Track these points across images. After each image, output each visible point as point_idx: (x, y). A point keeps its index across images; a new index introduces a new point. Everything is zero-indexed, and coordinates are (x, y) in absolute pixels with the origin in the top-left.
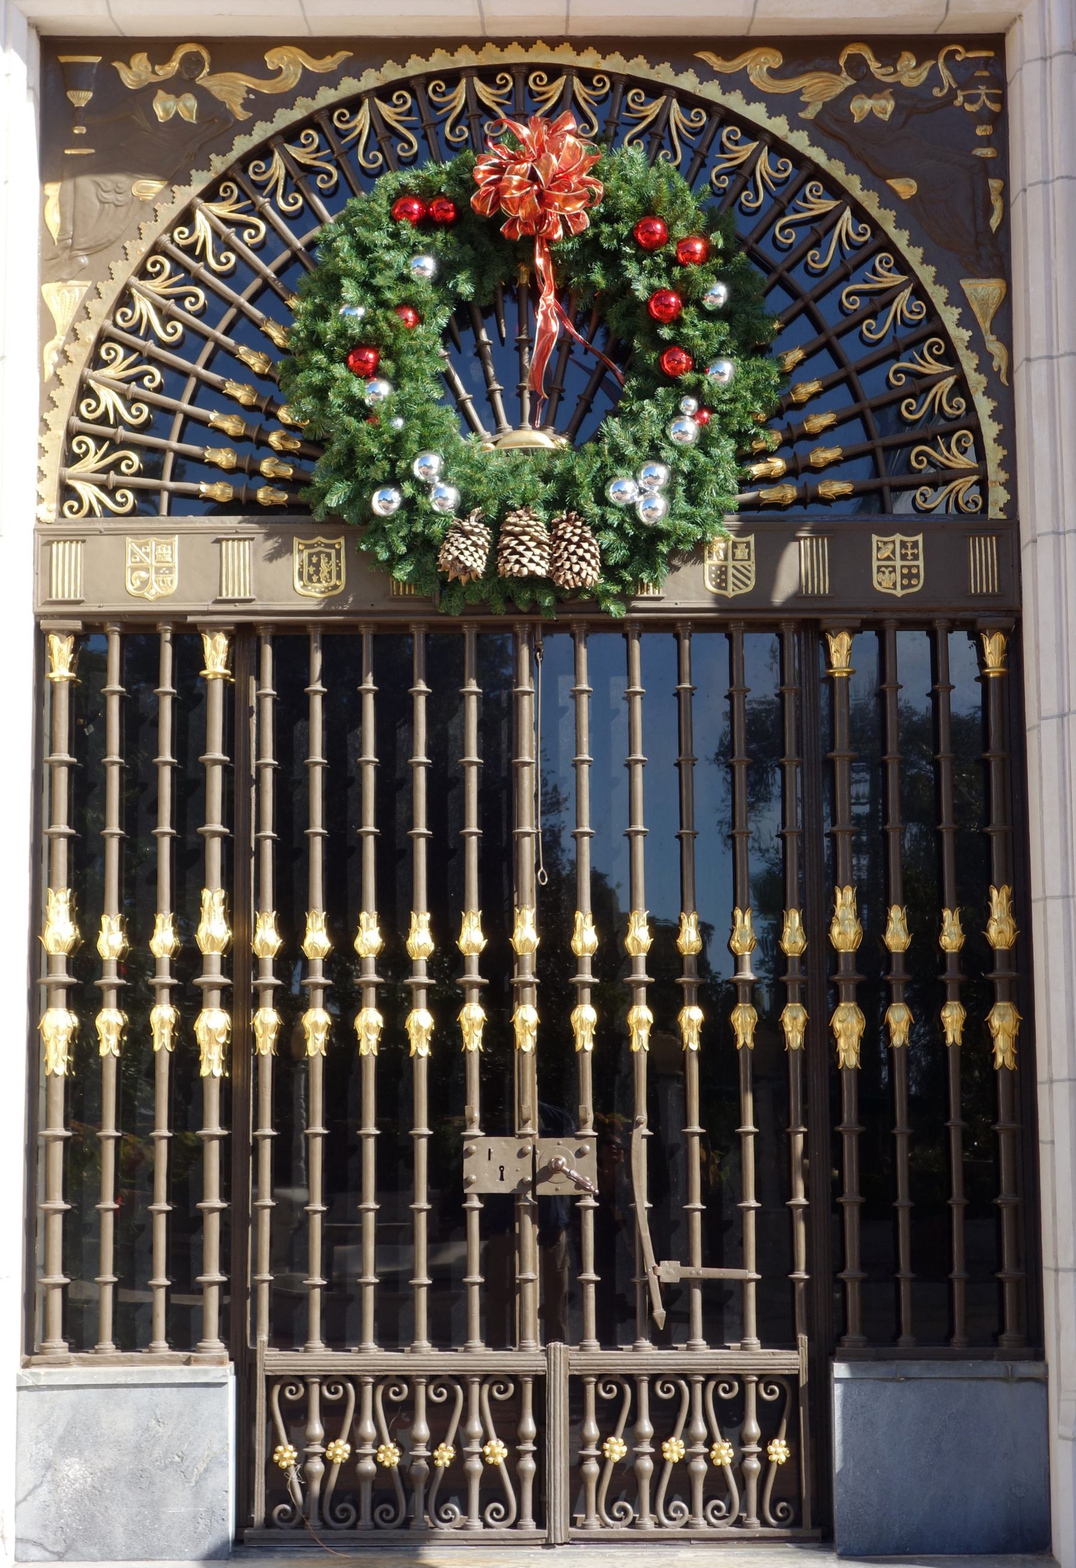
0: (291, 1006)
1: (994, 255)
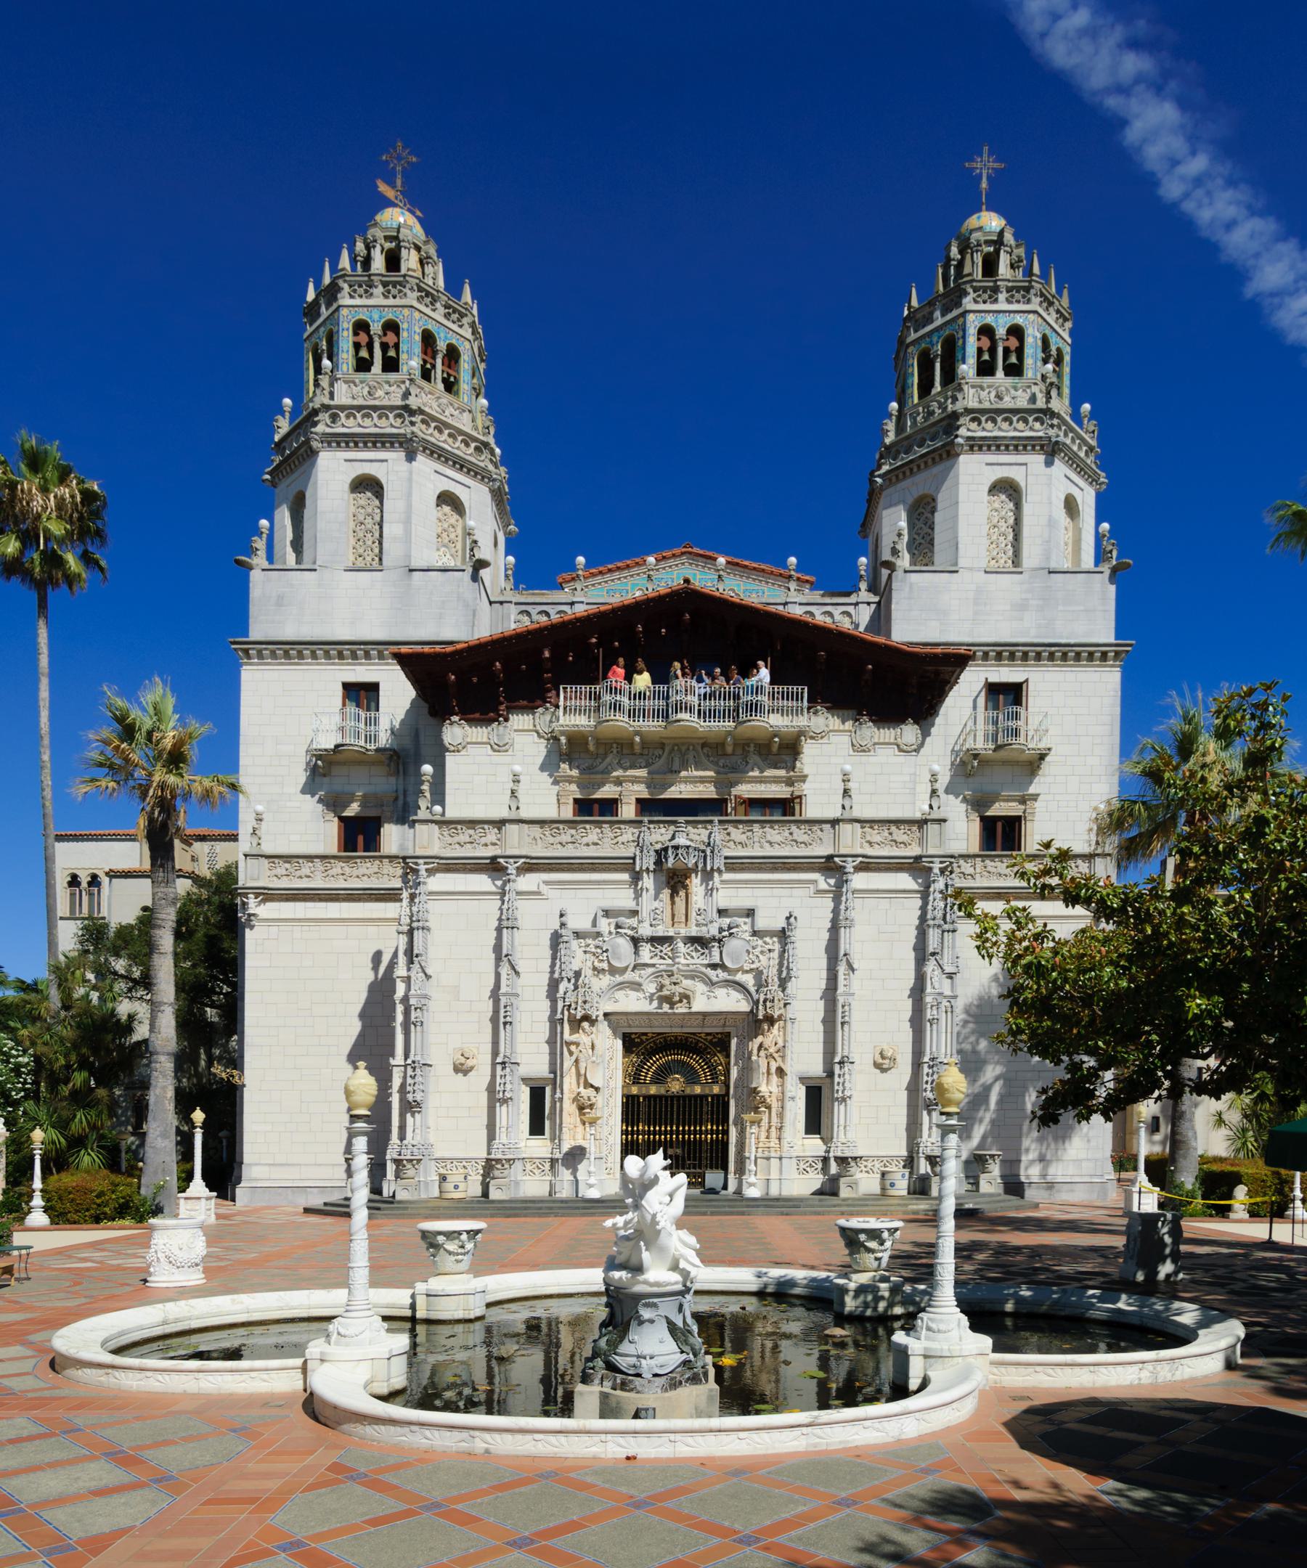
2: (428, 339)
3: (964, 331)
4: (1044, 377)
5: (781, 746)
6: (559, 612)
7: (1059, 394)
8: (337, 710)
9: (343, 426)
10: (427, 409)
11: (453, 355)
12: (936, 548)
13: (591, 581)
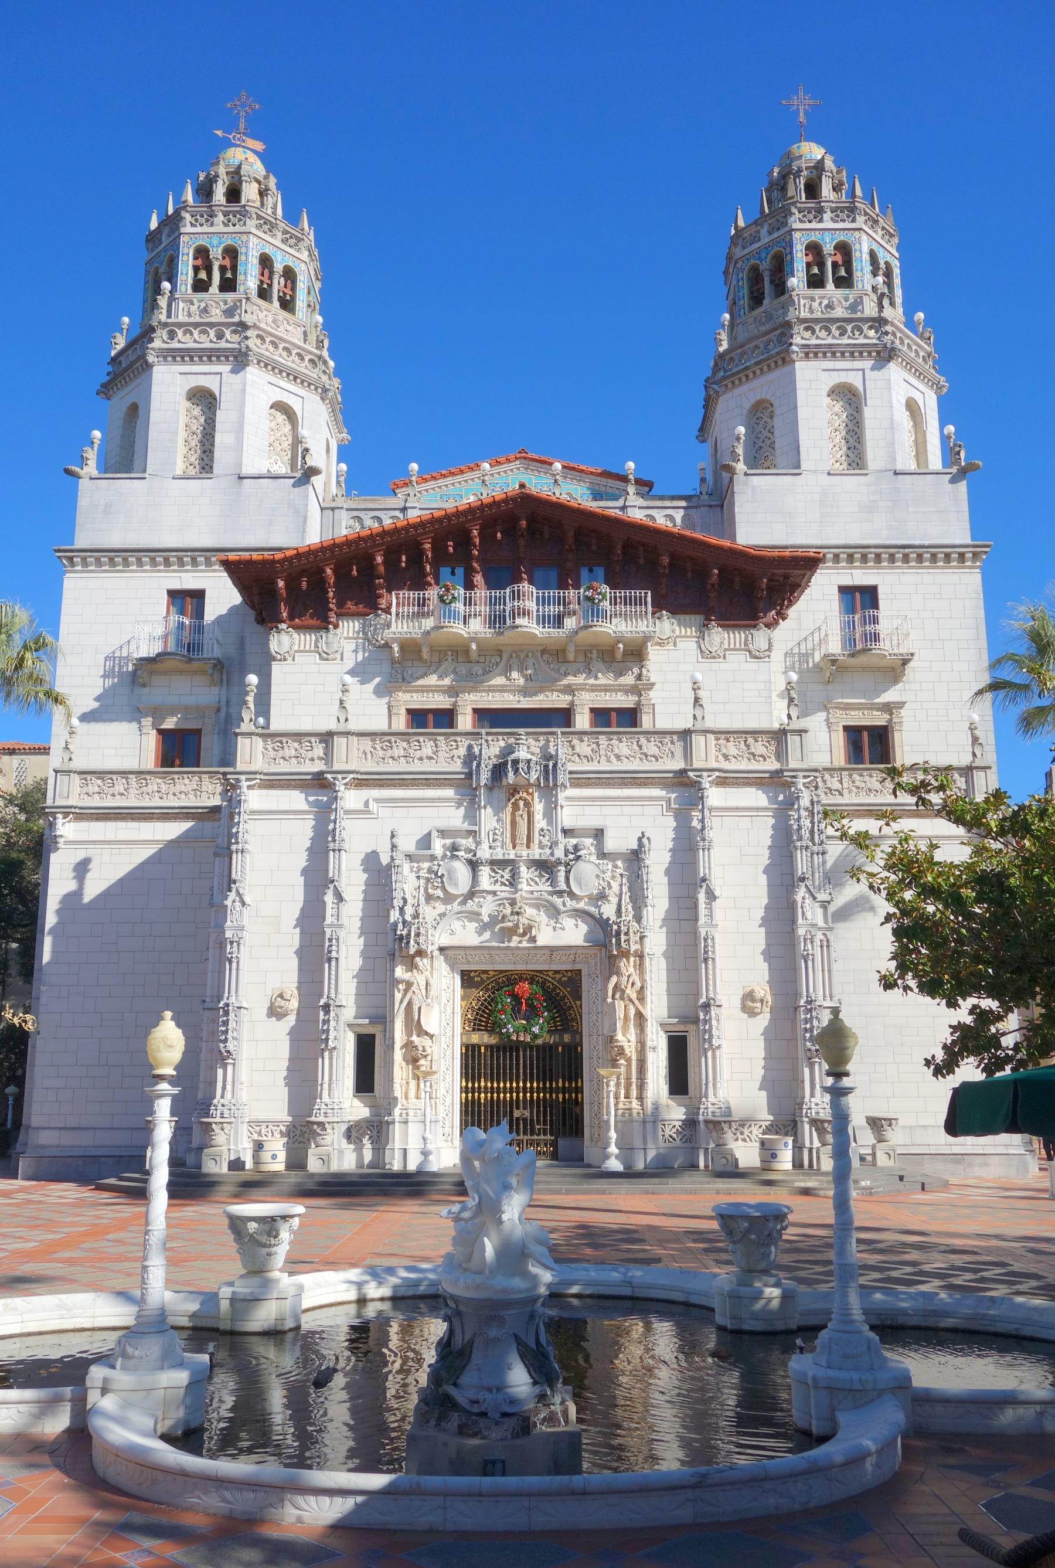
0: (492, 1093)
1: (580, 999)
2: (265, 261)
3: (791, 247)
4: (874, 289)
5: (625, 654)
6: (392, 517)
7: (891, 304)
8: (161, 618)
9: (179, 342)
10: (263, 325)
11: (289, 274)
12: (778, 452)
13: (424, 486)
